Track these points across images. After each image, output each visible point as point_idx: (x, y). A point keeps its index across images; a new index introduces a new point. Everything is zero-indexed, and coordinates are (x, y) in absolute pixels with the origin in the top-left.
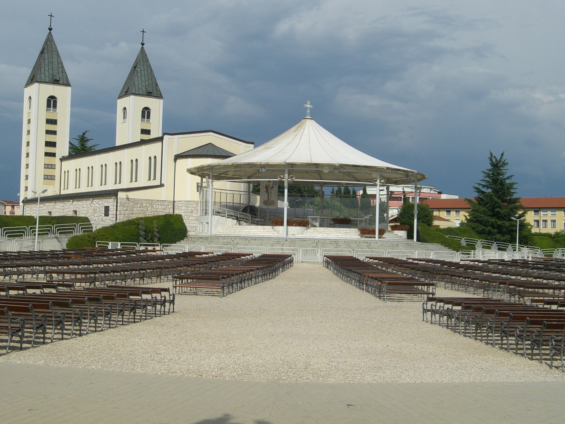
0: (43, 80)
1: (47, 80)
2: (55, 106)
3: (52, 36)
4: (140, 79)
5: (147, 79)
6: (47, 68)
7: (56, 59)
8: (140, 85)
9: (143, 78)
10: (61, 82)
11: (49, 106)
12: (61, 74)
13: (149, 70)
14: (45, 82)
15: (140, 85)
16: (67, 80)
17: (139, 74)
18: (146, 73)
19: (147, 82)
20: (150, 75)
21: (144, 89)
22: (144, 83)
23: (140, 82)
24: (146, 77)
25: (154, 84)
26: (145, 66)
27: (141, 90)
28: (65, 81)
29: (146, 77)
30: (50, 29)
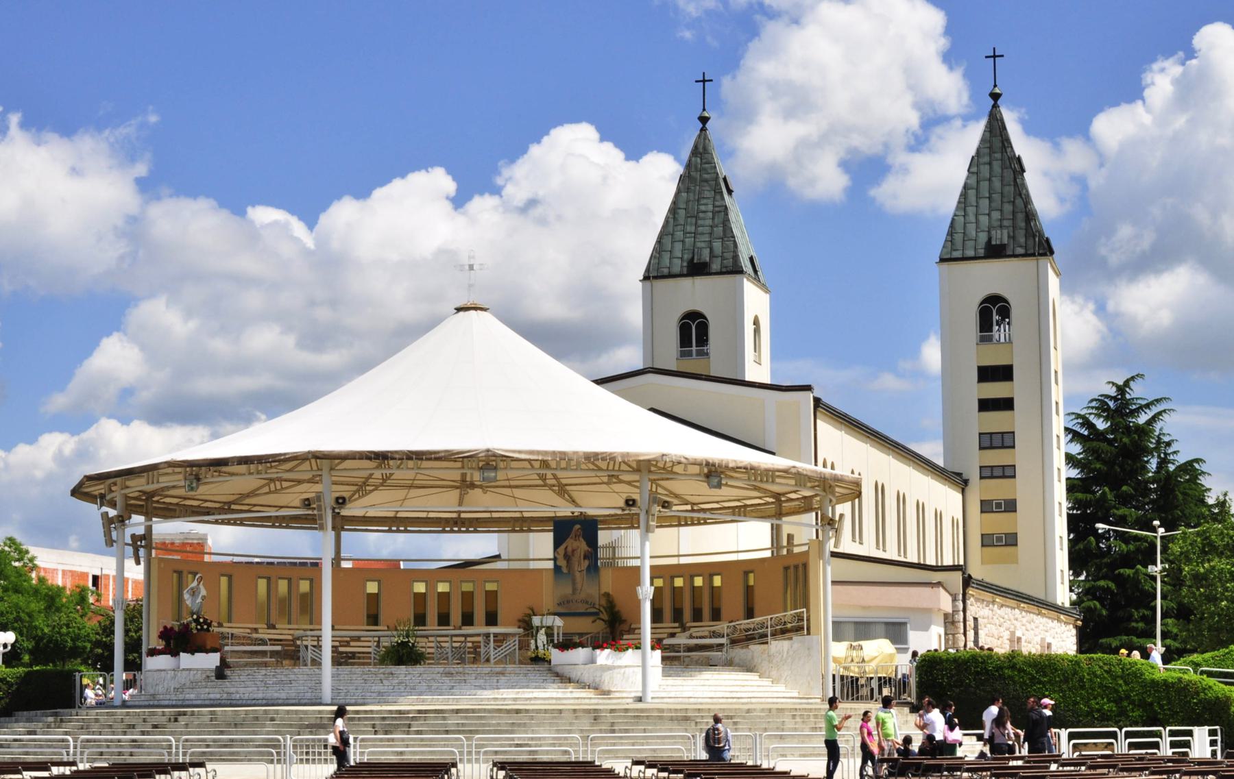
0: (666, 271)
1: (676, 269)
2: (703, 339)
3: (706, 138)
4: (971, 211)
5: (997, 204)
6: (679, 235)
7: (710, 201)
8: (971, 229)
9: (985, 203)
10: (715, 266)
11: (685, 341)
12: (717, 245)
13: (1009, 175)
14: (671, 276)
15: (971, 229)
16: (736, 257)
17: (972, 193)
18: (997, 184)
19: (996, 215)
20: (1010, 190)
21: (983, 237)
22: (984, 220)
23: (972, 218)
24: (996, 197)
25: (1021, 216)
26: (997, 166)
27: (970, 244)
28: (729, 263)
29: (996, 197)
30: (704, 120)
